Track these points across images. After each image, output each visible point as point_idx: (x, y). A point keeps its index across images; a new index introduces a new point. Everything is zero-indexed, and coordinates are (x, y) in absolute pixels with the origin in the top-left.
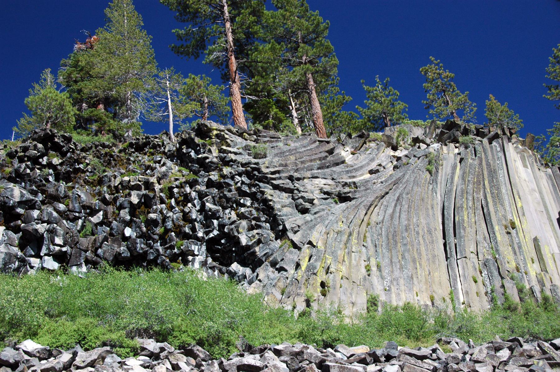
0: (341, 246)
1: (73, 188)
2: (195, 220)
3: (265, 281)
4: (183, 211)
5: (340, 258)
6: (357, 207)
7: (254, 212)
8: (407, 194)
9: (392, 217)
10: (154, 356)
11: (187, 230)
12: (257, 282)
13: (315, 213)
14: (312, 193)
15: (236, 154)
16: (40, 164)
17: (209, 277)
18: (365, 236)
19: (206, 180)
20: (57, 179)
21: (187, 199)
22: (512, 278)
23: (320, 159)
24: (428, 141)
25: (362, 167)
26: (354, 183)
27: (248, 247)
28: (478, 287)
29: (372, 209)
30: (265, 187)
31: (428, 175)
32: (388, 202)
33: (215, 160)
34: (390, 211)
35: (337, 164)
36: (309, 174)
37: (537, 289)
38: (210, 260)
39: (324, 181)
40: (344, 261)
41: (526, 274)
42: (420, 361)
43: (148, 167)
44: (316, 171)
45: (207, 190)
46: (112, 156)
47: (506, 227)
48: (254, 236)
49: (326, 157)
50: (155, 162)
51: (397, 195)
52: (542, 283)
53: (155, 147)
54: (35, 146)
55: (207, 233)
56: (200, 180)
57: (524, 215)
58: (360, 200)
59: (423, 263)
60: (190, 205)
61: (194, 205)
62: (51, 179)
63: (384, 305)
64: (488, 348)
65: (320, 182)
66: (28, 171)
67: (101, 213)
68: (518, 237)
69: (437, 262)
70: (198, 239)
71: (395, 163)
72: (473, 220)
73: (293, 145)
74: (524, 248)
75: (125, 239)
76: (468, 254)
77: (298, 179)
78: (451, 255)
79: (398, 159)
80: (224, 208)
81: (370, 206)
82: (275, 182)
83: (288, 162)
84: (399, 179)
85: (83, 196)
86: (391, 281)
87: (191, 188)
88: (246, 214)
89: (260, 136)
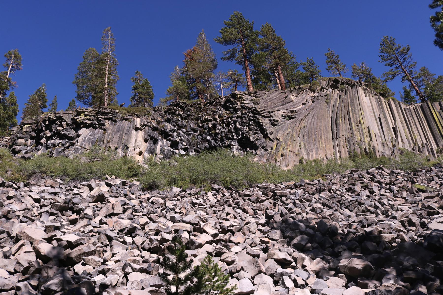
0: (289, 139)
1: (188, 122)
2: (233, 132)
3: (260, 155)
4: (228, 128)
5: (289, 144)
6: (296, 121)
7: (255, 127)
8: (317, 113)
9: (310, 123)
10: (217, 191)
11: (230, 136)
12: (257, 155)
13: (279, 126)
14: (278, 117)
15: (247, 103)
16: (176, 114)
17: (239, 153)
18: (299, 133)
19: (236, 115)
20: (182, 119)
21: (228, 124)
22: (358, 145)
23: (282, 101)
24: (327, 88)
25: (299, 102)
26: (295, 111)
27: (253, 142)
28: (345, 150)
29: (302, 121)
30: (259, 117)
31: (326, 104)
32: (309, 118)
33: (239, 107)
34: (310, 121)
35: (289, 102)
36: (276, 109)
37: (367, 148)
38: (239, 147)
39: (283, 111)
40: (290, 144)
41: (364, 142)
42: (312, 186)
43: (215, 111)
44: (280, 107)
45: (237, 120)
46: (201, 108)
47: (357, 123)
48: (255, 137)
49: (285, 100)
50: (217, 109)
51: (313, 114)
52: (370, 146)
53: (217, 103)
54: (174, 108)
55: (238, 137)
56: (234, 116)
57: (364, 118)
58: (297, 119)
59: (323, 142)
60: (230, 126)
61: (232, 126)
62: (180, 120)
63: (306, 160)
64: (340, 177)
65: (281, 112)
66: (172, 118)
67: (199, 131)
68: (362, 127)
69: (329, 141)
70: (235, 139)
71: (313, 99)
72: (344, 122)
73: (271, 96)
74: (364, 131)
75: (208, 141)
76: (341, 136)
77: (272, 112)
78: (334, 137)
79: (314, 97)
80: (244, 126)
81: (301, 120)
82: (263, 114)
83: (268, 105)
84: (314, 107)
85: (191, 125)
86: (309, 151)
87: (231, 119)
88: (252, 128)
89: (257, 94)
